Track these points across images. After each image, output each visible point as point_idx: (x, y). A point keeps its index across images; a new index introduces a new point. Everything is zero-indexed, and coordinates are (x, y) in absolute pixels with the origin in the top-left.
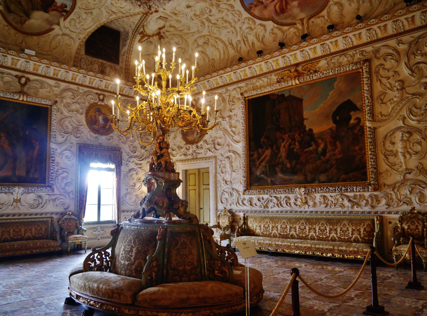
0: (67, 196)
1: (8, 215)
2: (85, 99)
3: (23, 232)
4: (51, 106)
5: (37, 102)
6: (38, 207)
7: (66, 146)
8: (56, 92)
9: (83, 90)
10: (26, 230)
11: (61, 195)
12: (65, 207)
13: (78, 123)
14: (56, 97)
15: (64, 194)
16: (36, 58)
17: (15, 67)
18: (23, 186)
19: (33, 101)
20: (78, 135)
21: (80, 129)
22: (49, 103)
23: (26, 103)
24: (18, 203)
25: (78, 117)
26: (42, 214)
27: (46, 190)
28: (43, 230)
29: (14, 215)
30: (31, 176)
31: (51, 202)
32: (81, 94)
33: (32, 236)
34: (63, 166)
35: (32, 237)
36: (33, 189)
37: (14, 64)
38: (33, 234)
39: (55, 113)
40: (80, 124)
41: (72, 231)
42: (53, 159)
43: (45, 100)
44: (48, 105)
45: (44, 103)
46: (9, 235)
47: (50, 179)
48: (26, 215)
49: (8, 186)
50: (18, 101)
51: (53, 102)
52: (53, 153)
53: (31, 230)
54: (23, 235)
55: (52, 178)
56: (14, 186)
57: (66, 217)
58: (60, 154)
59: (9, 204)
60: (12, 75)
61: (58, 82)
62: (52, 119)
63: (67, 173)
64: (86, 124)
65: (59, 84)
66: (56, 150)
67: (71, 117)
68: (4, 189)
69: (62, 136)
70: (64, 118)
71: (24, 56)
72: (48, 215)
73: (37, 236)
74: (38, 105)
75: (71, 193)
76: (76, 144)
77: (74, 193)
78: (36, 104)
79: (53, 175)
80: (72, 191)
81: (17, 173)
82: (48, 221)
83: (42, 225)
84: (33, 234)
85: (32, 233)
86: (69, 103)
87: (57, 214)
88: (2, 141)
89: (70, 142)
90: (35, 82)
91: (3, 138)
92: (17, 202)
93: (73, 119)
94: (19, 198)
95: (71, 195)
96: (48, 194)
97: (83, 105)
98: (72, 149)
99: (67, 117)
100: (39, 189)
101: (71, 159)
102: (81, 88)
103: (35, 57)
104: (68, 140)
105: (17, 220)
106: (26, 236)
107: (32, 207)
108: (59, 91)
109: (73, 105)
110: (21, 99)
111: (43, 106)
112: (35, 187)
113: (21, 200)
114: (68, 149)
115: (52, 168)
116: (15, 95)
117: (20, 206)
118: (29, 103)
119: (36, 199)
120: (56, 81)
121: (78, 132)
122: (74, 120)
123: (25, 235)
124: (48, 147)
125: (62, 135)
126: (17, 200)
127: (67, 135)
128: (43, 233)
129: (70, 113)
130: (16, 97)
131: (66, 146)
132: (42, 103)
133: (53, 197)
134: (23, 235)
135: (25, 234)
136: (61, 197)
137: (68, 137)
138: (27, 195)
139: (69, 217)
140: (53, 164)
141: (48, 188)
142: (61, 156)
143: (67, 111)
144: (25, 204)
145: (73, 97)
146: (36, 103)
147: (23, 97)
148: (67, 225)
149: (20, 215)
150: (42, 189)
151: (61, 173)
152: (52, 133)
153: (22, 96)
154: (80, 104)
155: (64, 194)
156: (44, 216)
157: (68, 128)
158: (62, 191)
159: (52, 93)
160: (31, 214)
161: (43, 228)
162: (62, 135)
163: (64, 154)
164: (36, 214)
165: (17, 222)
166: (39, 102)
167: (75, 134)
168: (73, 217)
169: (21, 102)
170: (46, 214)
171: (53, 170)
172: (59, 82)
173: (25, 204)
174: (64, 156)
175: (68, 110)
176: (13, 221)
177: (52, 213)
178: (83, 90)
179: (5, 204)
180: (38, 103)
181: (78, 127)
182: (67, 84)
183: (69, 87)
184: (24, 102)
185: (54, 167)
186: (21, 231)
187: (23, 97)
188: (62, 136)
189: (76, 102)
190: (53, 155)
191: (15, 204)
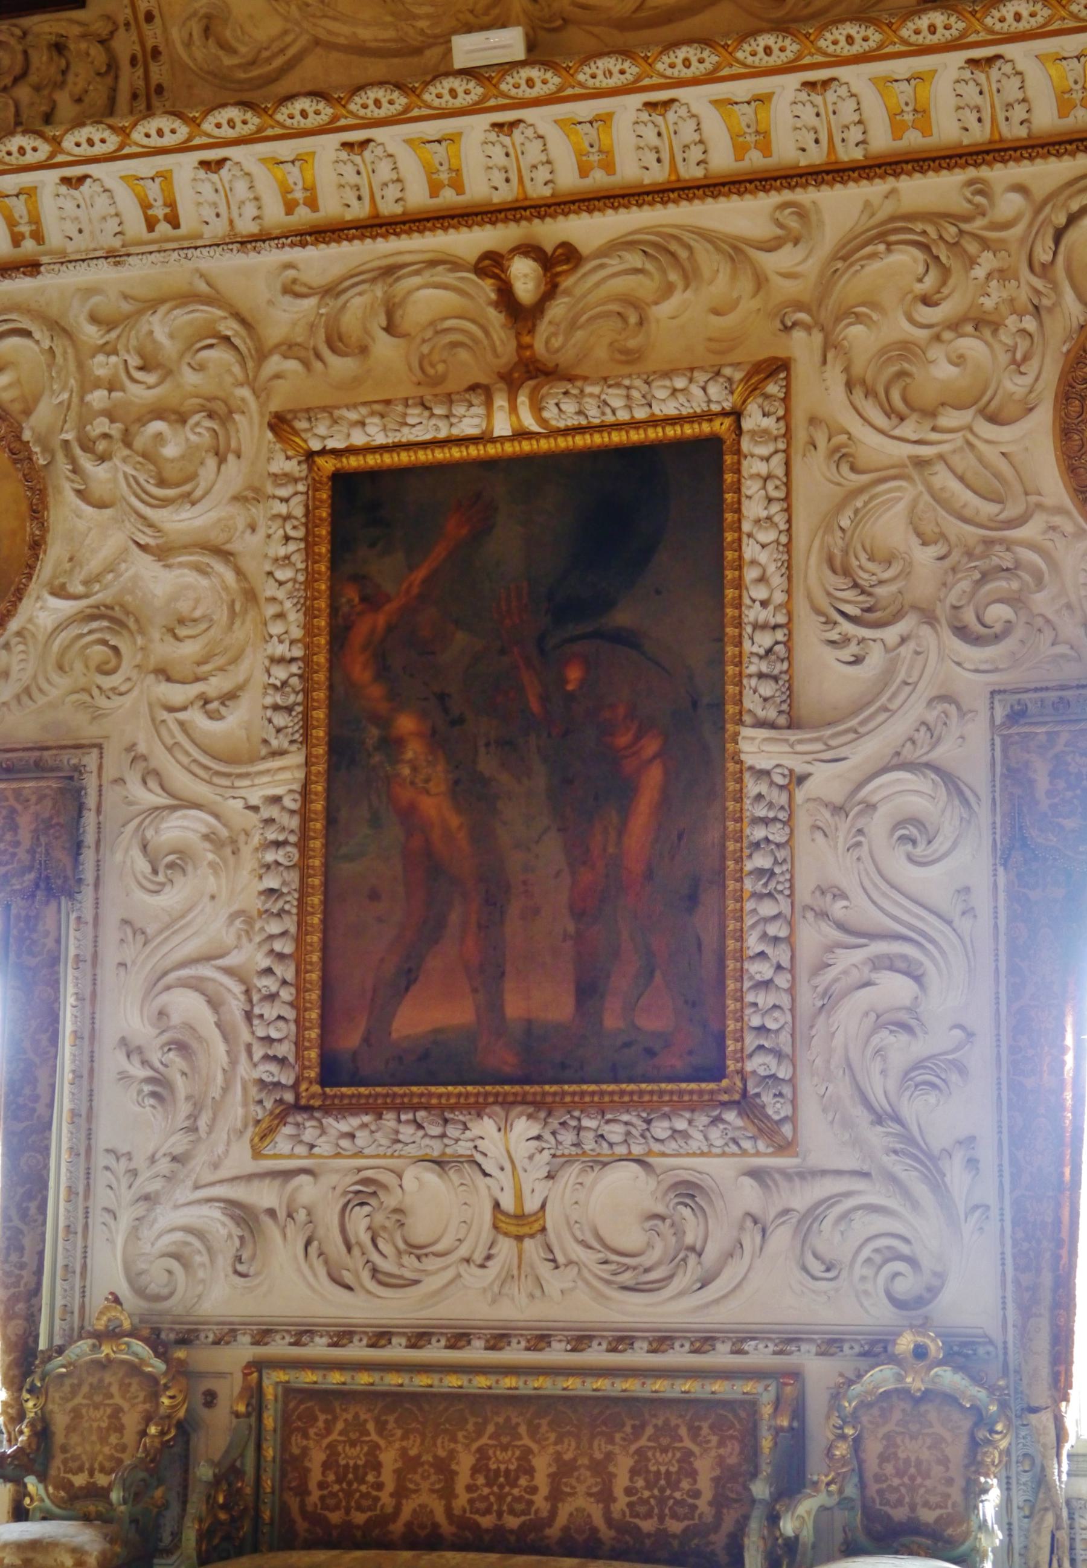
0: (921, 1190)
1: (459, 1338)
2: (1045, 271)
3: (541, 1480)
4: (736, 414)
5: (623, 416)
6: (671, 1277)
7: (897, 729)
8: (790, 289)
9: (1021, 189)
10: (563, 1470)
11: (866, 1175)
12: (904, 1287)
13: (989, 509)
14: (787, 329)
15: (889, 1161)
16: (534, 73)
17: (461, 200)
18: (540, 1107)
19: (594, 415)
20: (998, 613)
21: (1001, 558)
22: (719, 397)
23: (544, 445)
24: (528, 1243)
25: (991, 453)
26: (705, 1342)
27: (715, 1134)
28: (704, 1484)
29: (498, 1340)
30: (612, 1021)
31: (781, 1238)
32: (1018, 230)
33: (609, 1521)
34: (871, 917)
35: (606, 1534)
36: (614, 1133)
37: (444, 176)
38: (621, 1502)
39: (762, 468)
40: (1013, 510)
41: (928, 1516)
42: (761, 861)
43: (680, 383)
44: (708, 416)
45: (670, 409)
46: (447, 1493)
47: (751, 1041)
48: (580, 1341)
49: (443, 1112)
50: (492, 450)
51: (738, 376)
52: (761, 812)
53: (601, 1468)
54: (540, 1501)
55: (762, 1029)
56: (478, 1109)
57: (881, 1377)
58: (838, 810)
59: (463, 1251)
60: (454, 264)
61: (787, 195)
62: (746, 527)
63: (918, 979)
64: (1068, 502)
65: (801, 213)
66: (801, 779)
67: (920, 463)
68: (407, 1132)
69: (846, 654)
70: (861, 490)
71: (453, 93)
72: (759, 1356)
73: (647, 1526)
74: (636, 436)
75: (959, 1157)
76: (982, 705)
77: (987, 1154)
78: (617, 438)
79: (762, 999)
80: (969, 1141)
81: (515, 1007)
82: (751, 1405)
83: (695, 1432)
84: (621, 1502)
85: (606, 1496)
86: (906, 349)
87: (831, 1345)
88: (406, 771)
89: (926, 690)
90: (614, 264)
91: (413, 750)
92: (519, 1238)
93: (943, 478)
94: (531, 1205)
95: (956, 1175)
96: (756, 1174)
97: (1030, 323)
98: (940, 754)
99: (896, 472)
100: (660, 1129)
101: (941, 845)
102: (999, 175)
103: (526, 73)
104: (902, 676)
105: (509, 1382)
106: (565, 1511)
107: (626, 1278)
108: (811, 267)
109: (936, 352)
110: (502, 426)
111: (671, 432)
112: (627, 1107)
113: (552, 1219)
114: (908, 753)
115: (753, 943)
116: (459, 410)
117: (545, 1270)
118: (562, 443)
119: (660, 1209)
120: (774, 198)
121: (1000, 585)
122: (955, 485)
123: (553, 1513)
124: (731, 766)
125: (846, 640)
126: (520, 1217)
127: (890, 634)
128: (703, 1504)
129: (908, 429)
130: (469, 425)
131: (897, 729)
132: (658, 410)
133: (802, 1197)
134: (386, 1498)
135: (556, 1496)
136: (872, 1194)
137: (906, 651)
138: (589, 1178)
139: (914, 1382)
140: (767, 909)
141: (731, 1116)
142: (844, 825)
143: (880, 420)
144: (579, 1253)
145: (930, 282)
146: (618, 426)
147: (513, 409)
148: (883, 1458)
149: (540, 1340)
150: (681, 1124)
151: (855, 976)
152: (747, 645)
153: (500, 401)
154: (996, 327)
155: (889, 1161)
156: (721, 1357)
157: (907, 572)
158: (877, 1137)
159: (748, 305)
160: (622, 1341)
161: (705, 1468)
162: (846, 640)
163: (870, 807)
164: (662, 1341)
165: (513, 1400)
166: (641, 414)
167: (969, 617)
168: (949, 1378)
169: (509, 448)
170: (739, 1342)
171: (762, 955)
172: (806, 196)
173: (579, 1253)
174: (878, 825)
175: (890, 412)
176: (482, 1382)
177: (789, 1340)
178: (1021, 189)
179: (438, 1248)
180: (635, 424)
181: (989, 543)
182: (874, 190)
183: (888, 208)
184: (526, 446)
185: (772, 930)
186: (530, 1471)
187: (513, 409)
188: (846, 654)
189: (955, 326)
190: (759, 833)
191: (505, 1247)
